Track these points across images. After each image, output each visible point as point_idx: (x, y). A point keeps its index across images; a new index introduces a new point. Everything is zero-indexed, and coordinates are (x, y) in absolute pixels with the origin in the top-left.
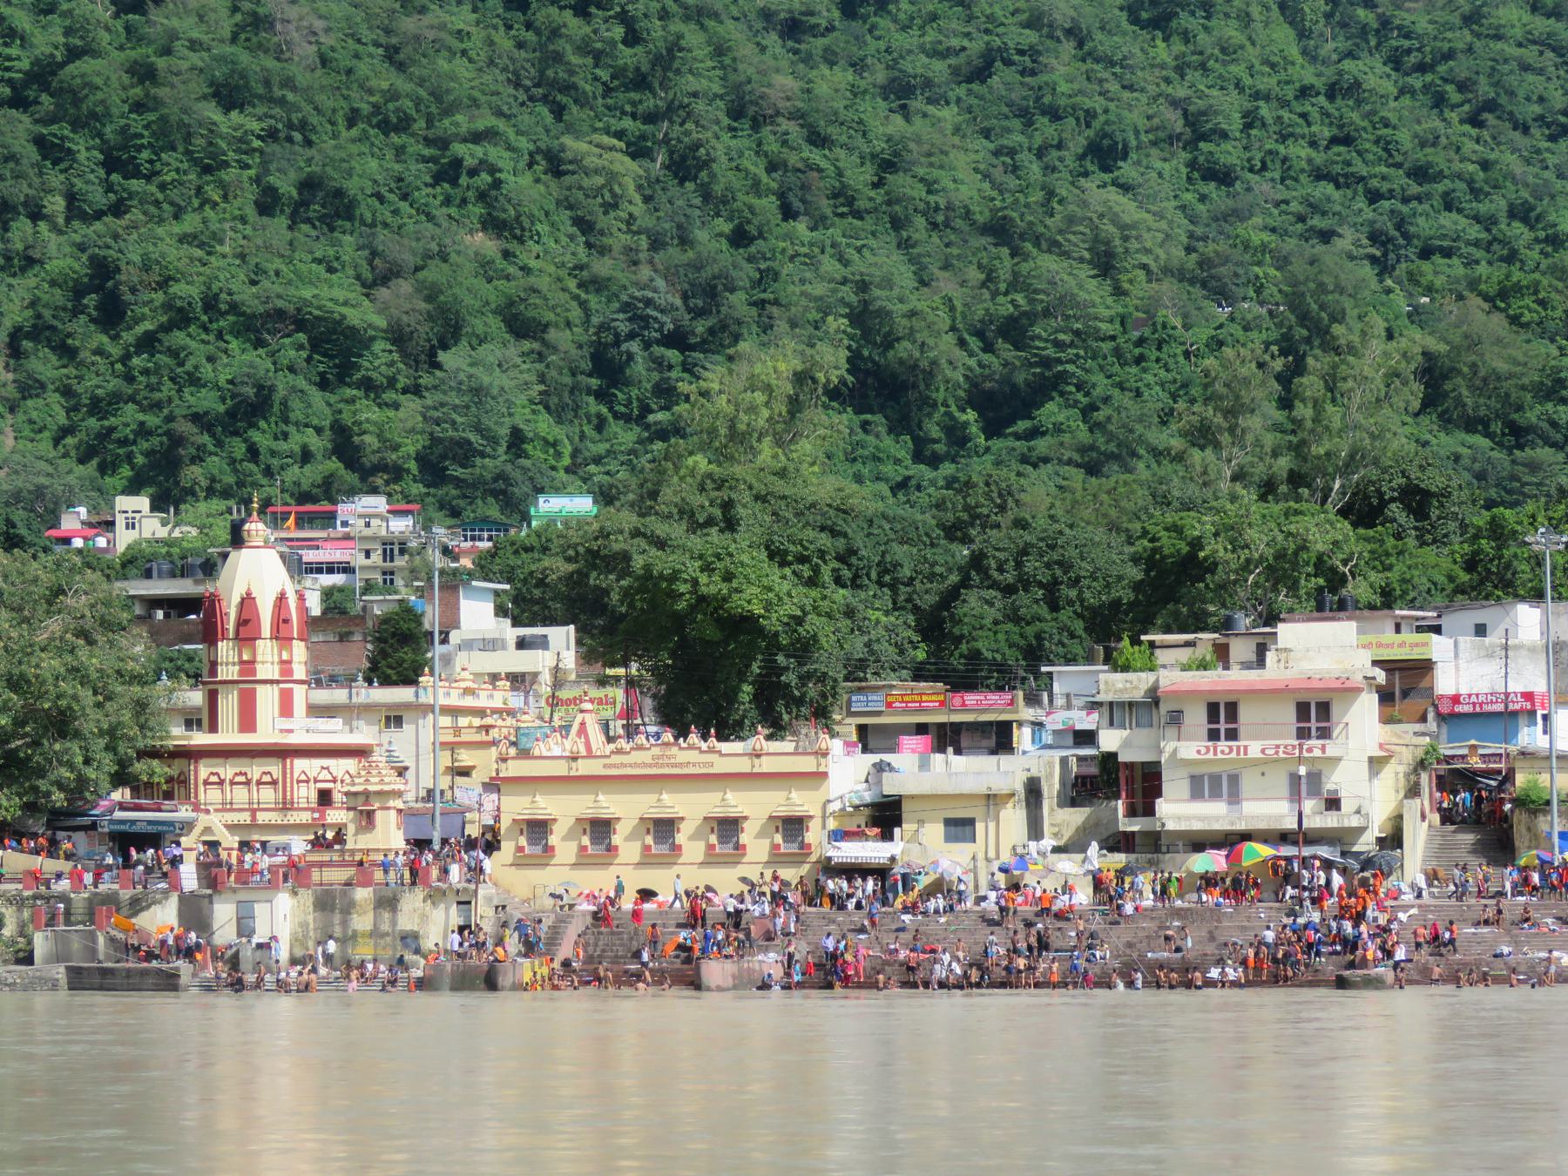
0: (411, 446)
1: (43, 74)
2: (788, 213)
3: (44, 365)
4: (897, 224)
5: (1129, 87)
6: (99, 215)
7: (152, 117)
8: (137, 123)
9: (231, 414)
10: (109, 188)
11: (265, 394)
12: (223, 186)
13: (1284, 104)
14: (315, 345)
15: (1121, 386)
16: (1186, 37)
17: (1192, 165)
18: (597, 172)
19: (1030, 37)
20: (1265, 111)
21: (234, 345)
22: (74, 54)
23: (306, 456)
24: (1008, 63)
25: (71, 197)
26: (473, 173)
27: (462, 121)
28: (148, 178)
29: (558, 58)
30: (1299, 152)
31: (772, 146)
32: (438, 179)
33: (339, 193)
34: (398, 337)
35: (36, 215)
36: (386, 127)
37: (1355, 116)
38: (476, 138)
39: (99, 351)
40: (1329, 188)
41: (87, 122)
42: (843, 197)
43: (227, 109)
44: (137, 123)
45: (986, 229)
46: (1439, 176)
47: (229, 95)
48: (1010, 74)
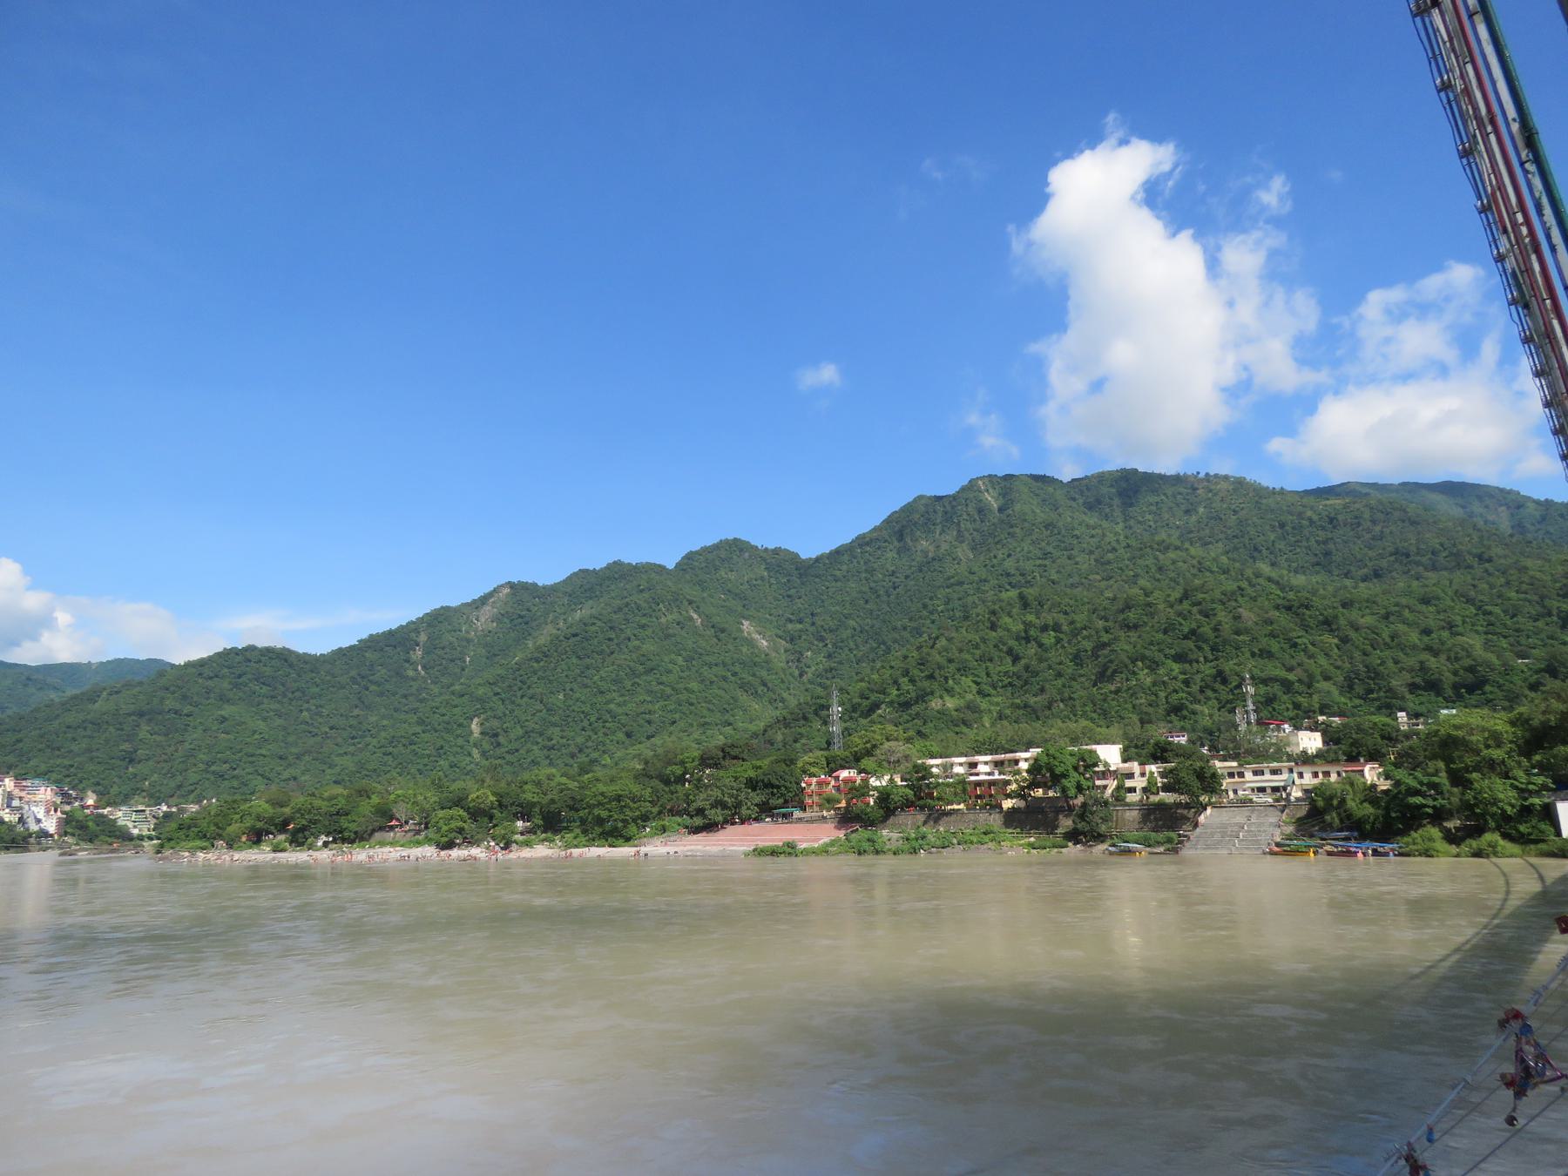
0: (1317, 706)
1: (1193, 632)
2: (1375, 649)
3: (1209, 693)
4: (1402, 650)
5: (1426, 618)
6: (1212, 661)
7: (1221, 639)
8: (1217, 640)
9: (1266, 701)
10: (1213, 655)
11: (1275, 695)
12: (1242, 652)
13: (1471, 618)
14: (1281, 684)
15: (1506, 681)
16: (1435, 605)
17: (1452, 633)
18: (1327, 643)
19: (1397, 609)
20: (1468, 620)
21: (1261, 686)
22: (1199, 627)
23: (1288, 709)
24: (1393, 615)
25: (1205, 658)
26: (1301, 645)
27: (1294, 634)
28: (1223, 652)
29: (1305, 620)
30: (1480, 628)
31: (1364, 635)
32: (1291, 647)
33: (1270, 652)
34: (1300, 681)
35: (1197, 662)
36: (1274, 637)
37: (1493, 619)
38: (1299, 637)
39: (1223, 690)
40: (1490, 636)
41: (1206, 641)
42: (1385, 644)
43: (1239, 636)
44: (1217, 640)
45: (1424, 649)
46: (1523, 631)
47: (1238, 633)
48: (1394, 617)
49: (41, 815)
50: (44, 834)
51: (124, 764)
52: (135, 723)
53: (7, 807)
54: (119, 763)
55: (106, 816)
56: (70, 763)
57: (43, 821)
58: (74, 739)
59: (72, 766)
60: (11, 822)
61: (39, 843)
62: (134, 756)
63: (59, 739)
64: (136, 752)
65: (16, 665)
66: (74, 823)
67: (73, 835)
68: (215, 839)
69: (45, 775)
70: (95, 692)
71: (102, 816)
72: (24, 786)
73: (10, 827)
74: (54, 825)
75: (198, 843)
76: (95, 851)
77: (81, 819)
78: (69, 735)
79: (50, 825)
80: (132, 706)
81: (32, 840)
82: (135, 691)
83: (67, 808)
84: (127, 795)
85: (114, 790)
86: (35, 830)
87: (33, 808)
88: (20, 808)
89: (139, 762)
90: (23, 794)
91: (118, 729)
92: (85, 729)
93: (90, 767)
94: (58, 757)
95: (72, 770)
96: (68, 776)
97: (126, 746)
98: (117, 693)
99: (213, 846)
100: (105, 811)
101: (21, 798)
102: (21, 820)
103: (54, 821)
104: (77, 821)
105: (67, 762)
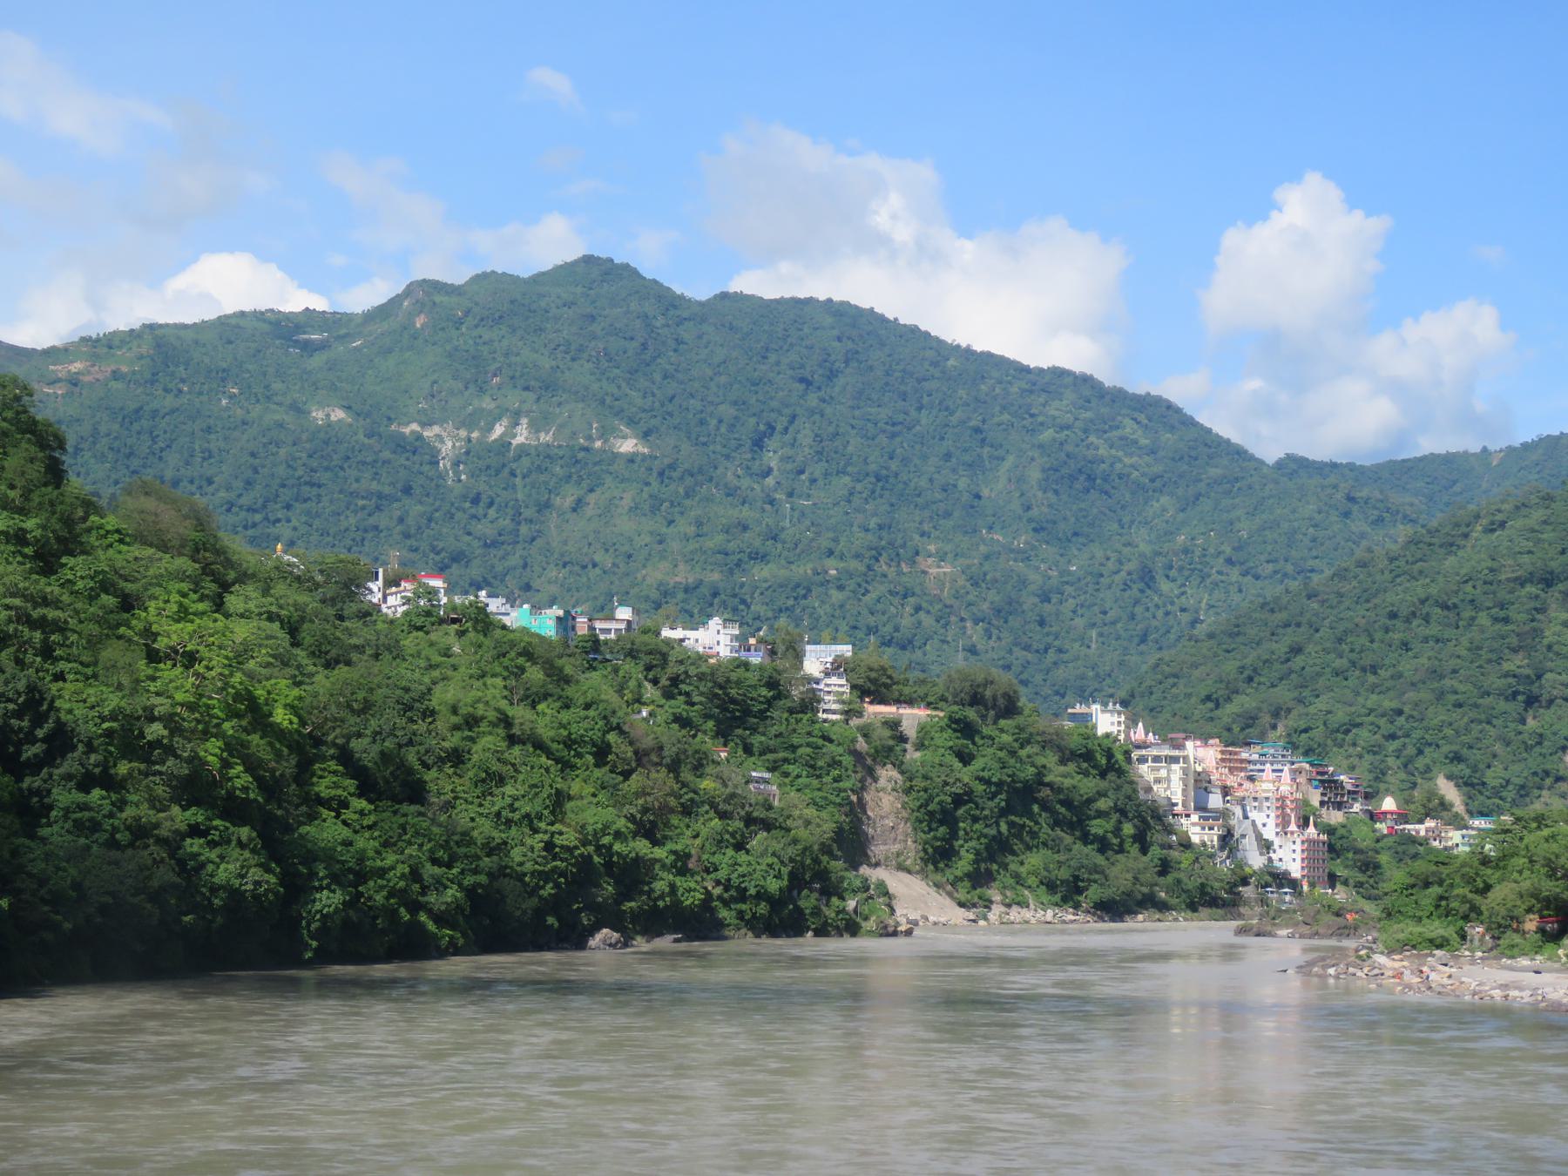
49: (1269, 833)
50: (1281, 879)
51: (1514, 708)
52: (1533, 604)
53: (1197, 809)
54: (1502, 705)
55: (1424, 842)
56: (1394, 704)
57: (1276, 846)
58: (1406, 646)
59: (1400, 712)
60: (1204, 844)
61: (1264, 902)
62: (1535, 689)
63: (1375, 646)
64: (1539, 677)
65: (1334, 466)
66: (1350, 855)
67: (1345, 883)
68: (1466, 918)
69: (1347, 732)
70: (1457, 525)
71: (1412, 840)
72: (1242, 761)
73: (1200, 854)
74: (1298, 856)
75: (1436, 928)
76: (1306, 930)
77: (1363, 845)
78: (1396, 636)
79: (1291, 858)
80: (1526, 559)
81: (1248, 892)
82: (1538, 515)
83: (1335, 817)
84: (1523, 787)
85: (1493, 777)
86: (1256, 867)
87: (1253, 815)
88: (1224, 814)
89: (1551, 702)
90: (1231, 781)
91: (1496, 620)
92: (1427, 619)
93: (1437, 715)
94: (1373, 689)
95: (1401, 720)
96: (1393, 737)
97: (1516, 663)
98: (1502, 524)
99: (1463, 937)
100: (1421, 829)
101: (1226, 791)
102: (1227, 839)
103: (1298, 847)
104: (1357, 851)
105: (1388, 704)
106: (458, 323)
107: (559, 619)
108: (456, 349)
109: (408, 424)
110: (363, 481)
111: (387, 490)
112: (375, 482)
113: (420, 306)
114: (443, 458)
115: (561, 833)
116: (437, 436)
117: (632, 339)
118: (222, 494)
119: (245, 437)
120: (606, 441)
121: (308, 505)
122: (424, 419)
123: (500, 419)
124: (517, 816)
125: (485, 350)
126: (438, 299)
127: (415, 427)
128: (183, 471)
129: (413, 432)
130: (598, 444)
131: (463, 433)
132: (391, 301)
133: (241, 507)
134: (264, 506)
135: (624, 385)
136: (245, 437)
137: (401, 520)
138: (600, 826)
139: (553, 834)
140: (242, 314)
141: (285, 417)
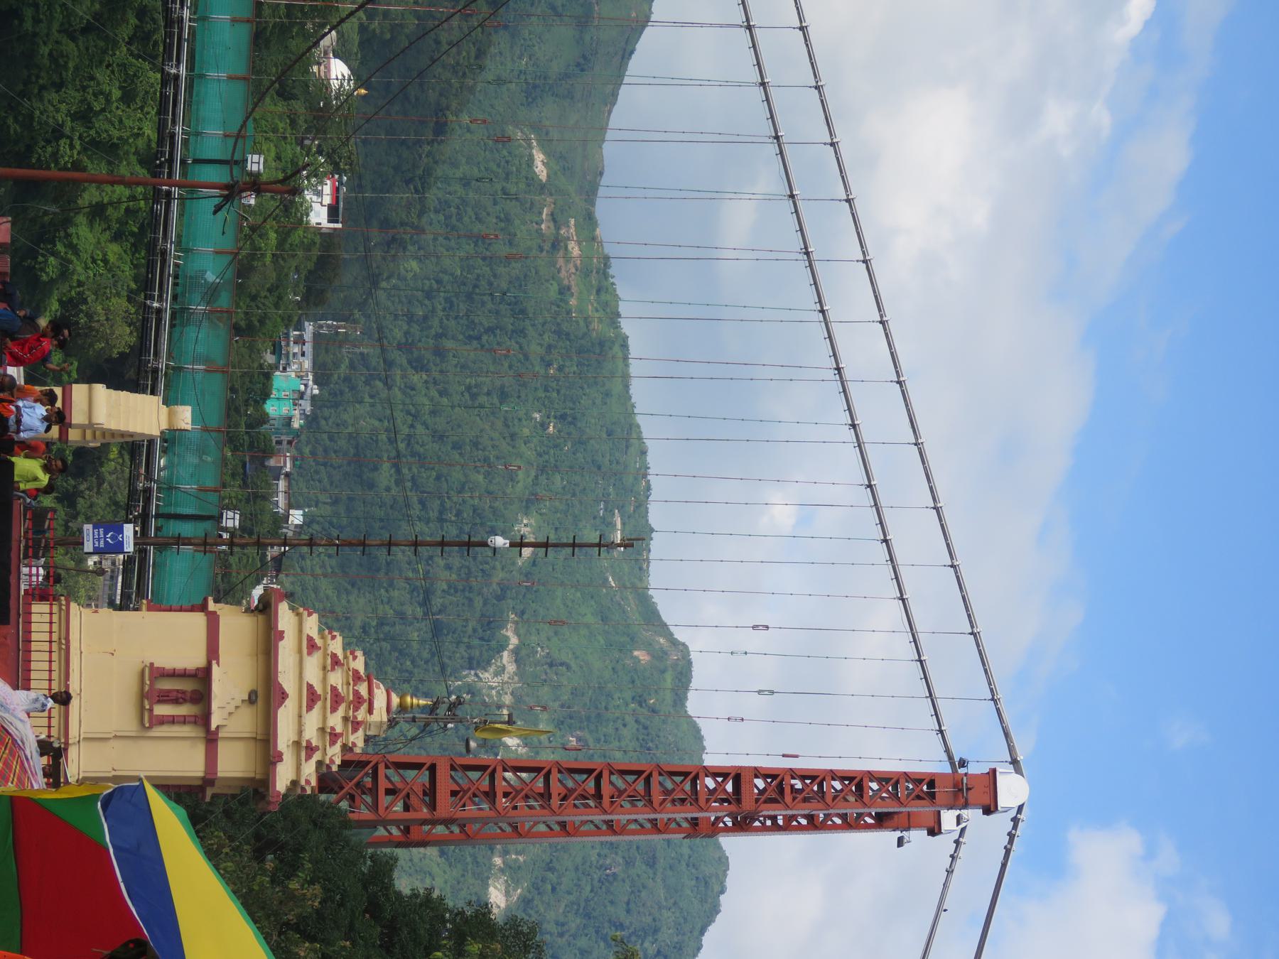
106: (641, 702)
107: (289, 420)
108: (609, 695)
109: (517, 633)
110: (447, 573)
111: (437, 602)
112: (445, 587)
113: (659, 656)
114: (476, 675)
115: (72, 147)
116: (504, 668)
117: (628, 911)
118: (427, 407)
119: (496, 435)
120: (502, 871)
121: (417, 506)
122: (523, 652)
123: (526, 745)
124: (90, 97)
125: (610, 729)
126: (669, 677)
127: (514, 641)
128: (455, 361)
129: (507, 639)
130: (498, 861)
131: (507, 699)
132: (664, 626)
133: (412, 426)
134: (413, 454)
135: (572, 898)
136: (496, 435)
137: (402, 616)
138: (75, 241)
139: (71, 139)
140: (644, 453)
141: (520, 485)
